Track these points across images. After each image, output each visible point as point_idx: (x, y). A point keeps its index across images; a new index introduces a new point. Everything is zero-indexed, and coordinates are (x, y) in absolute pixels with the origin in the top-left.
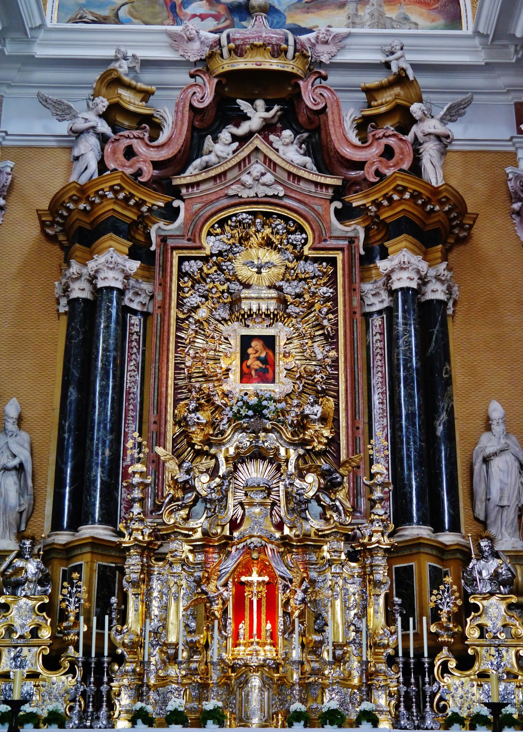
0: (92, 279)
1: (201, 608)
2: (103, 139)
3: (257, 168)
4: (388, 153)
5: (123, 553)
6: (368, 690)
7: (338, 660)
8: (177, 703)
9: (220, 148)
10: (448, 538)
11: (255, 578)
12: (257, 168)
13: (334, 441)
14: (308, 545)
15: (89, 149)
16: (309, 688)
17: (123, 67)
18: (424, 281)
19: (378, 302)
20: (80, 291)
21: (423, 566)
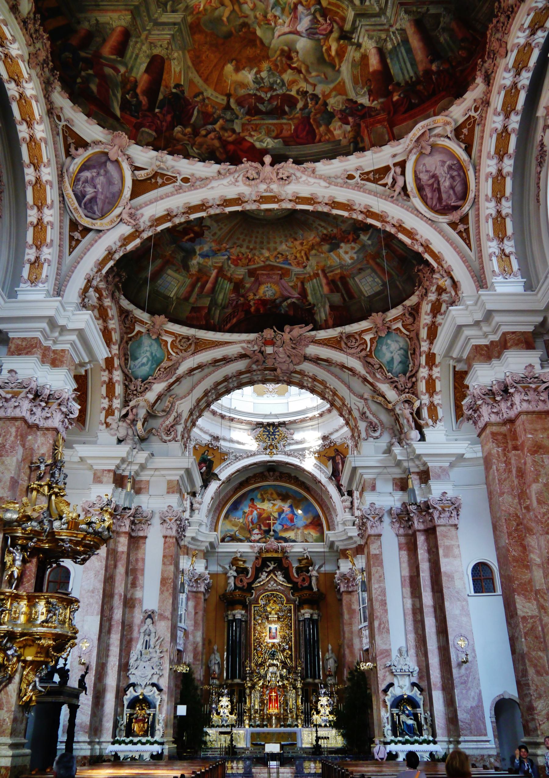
0: (234, 616)
1: (262, 702)
2: (235, 577)
3: (272, 583)
4: (304, 580)
5: (245, 689)
6: (297, 719)
7: (291, 712)
8: (258, 723)
9: (264, 576)
10: (317, 681)
11: (273, 694)
12: (272, 583)
13: (291, 655)
14: (284, 686)
15: (231, 581)
16: (285, 719)
17: (238, 555)
18: (312, 615)
19: (301, 619)
20: (230, 618)
21: (310, 689)
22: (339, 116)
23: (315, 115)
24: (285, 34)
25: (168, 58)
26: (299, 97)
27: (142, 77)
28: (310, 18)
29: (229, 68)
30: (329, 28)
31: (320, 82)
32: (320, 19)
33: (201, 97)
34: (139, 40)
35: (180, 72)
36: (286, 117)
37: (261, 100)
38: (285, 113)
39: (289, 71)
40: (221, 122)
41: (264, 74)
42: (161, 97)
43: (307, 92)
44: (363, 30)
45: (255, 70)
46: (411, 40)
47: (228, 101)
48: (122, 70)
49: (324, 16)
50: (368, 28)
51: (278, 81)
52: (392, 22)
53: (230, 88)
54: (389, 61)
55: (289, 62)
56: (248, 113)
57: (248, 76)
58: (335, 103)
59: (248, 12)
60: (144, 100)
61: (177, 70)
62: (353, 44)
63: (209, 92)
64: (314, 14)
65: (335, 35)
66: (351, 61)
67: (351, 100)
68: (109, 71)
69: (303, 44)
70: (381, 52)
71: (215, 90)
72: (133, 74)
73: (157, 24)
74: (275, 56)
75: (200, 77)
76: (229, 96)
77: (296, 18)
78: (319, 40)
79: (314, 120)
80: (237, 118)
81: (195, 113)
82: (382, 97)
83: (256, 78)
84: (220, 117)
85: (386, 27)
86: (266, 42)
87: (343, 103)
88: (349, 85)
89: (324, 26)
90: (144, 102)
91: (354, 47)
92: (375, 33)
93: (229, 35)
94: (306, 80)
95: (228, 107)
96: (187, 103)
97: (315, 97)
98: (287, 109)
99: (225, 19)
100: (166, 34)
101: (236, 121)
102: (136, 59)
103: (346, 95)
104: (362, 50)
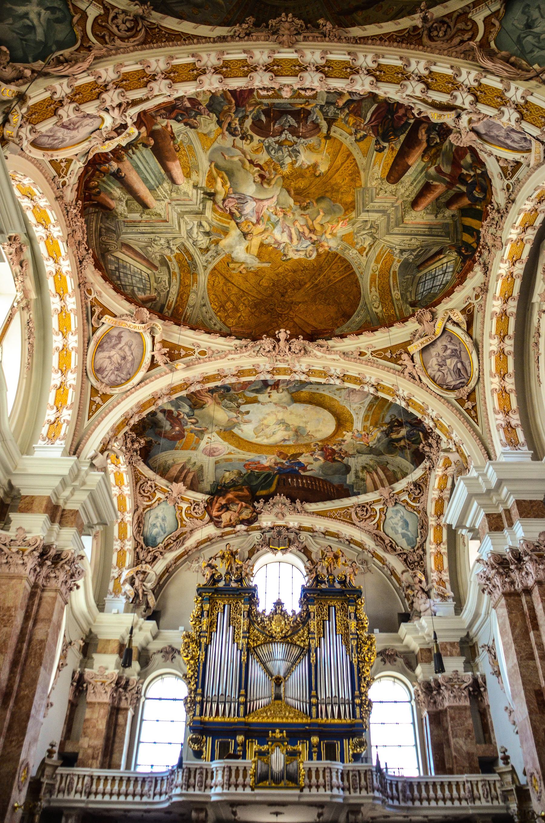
22: (201, 107)
23: (230, 109)
24: (267, 199)
25: (382, 179)
26: (250, 132)
27: (415, 162)
28: (245, 212)
29: (323, 168)
30: (226, 203)
31: (228, 149)
32: (235, 211)
33: (359, 136)
34: (405, 199)
35: (374, 165)
36: (264, 107)
37: (294, 131)
38: (266, 113)
39: (262, 163)
40: (341, 103)
41: (288, 160)
42: (402, 137)
43: (242, 138)
44: (195, 201)
45: (297, 165)
46: (148, 191)
47: (329, 130)
48: (432, 170)
49: (232, 214)
50: (191, 203)
51: (273, 152)
52: (170, 207)
53: (326, 146)
54: (163, 171)
55: (262, 172)
56: (308, 113)
57: (305, 158)
58: (208, 123)
59: (300, 218)
60: (422, 135)
61: (376, 167)
62: (201, 188)
63: (348, 141)
64: (242, 215)
65: (219, 198)
66: (201, 173)
67: (192, 127)
68: (447, 169)
69: (250, 189)
70: (173, 181)
71: (342, 144)
72: (423, 164)
73: (384, 212)
74: (276, 179)
75: (354, 159)
76: (328, 137)
77: (257, 212)
78: (235, 193)
79: (230, 102)
80: (322, 106)
81: (369, 115)
82: (158, 131)
83: (296, 156)
84: (342, 109)
85: (174, 203)
86: (285, 193)
87: (200, 123)
88: (197, 146)
89: (231, 204)
90: (423, 131)
91: (199, 186)
92: (183, 198)
93: (319, 200)
94: (244, 152)
95: (330, 122)
96: (375, 129)
97: (233, 133)
98: (263, 118)
99: (322, 214)
100: (378, 203)
101: (323, 103)
102: (415, 180)
103: (198, 133)
104: (191, 182)
